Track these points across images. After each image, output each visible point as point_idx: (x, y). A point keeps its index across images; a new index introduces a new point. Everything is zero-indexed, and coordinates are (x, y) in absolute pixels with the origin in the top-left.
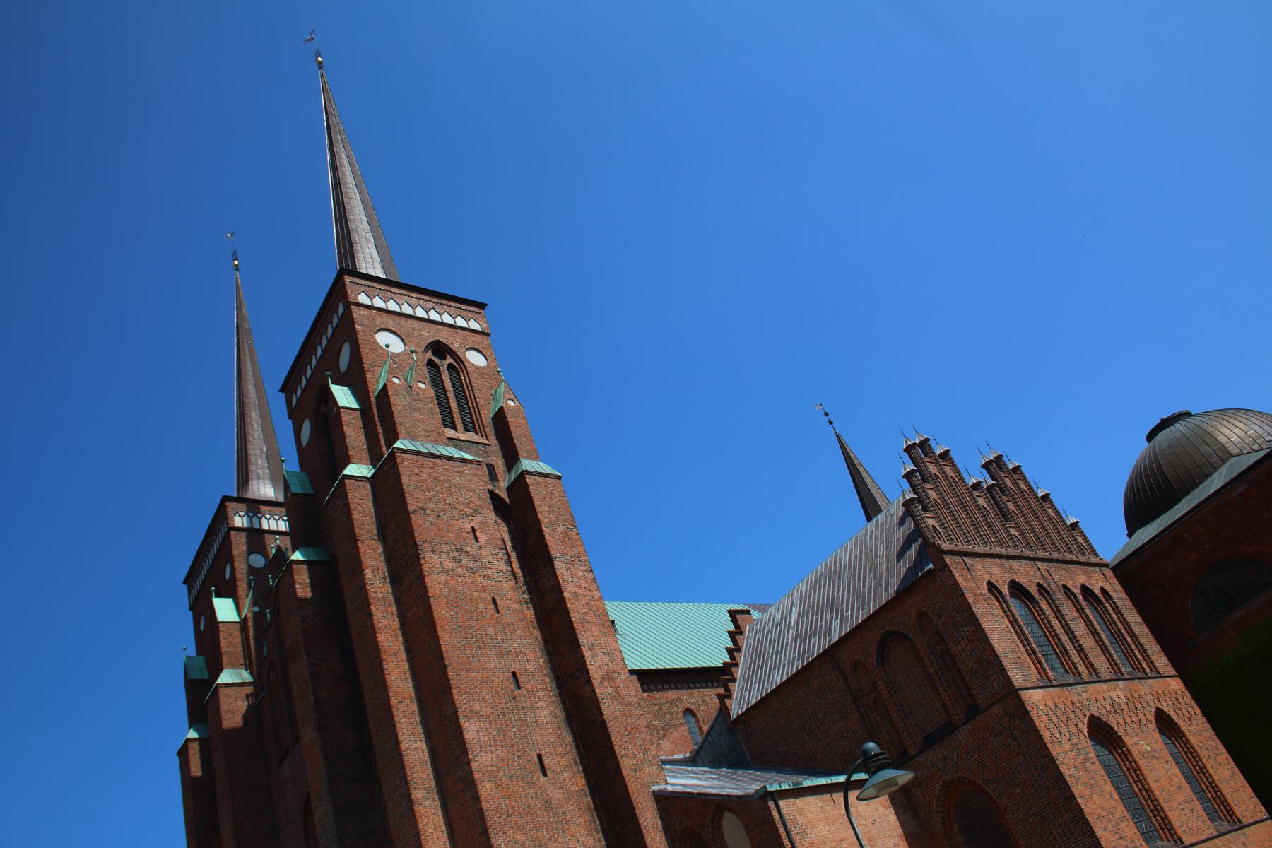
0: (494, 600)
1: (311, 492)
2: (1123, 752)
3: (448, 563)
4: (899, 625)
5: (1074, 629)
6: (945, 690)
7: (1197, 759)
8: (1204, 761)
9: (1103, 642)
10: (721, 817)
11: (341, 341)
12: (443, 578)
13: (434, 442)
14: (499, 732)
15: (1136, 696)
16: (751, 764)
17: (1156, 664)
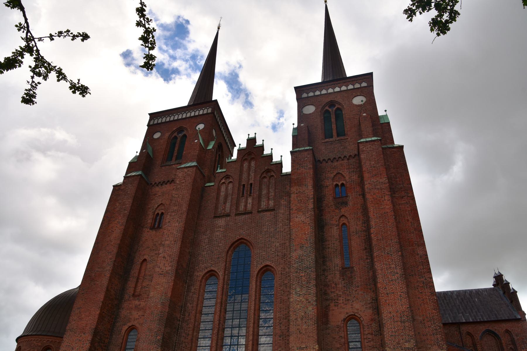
11: (359, 94)
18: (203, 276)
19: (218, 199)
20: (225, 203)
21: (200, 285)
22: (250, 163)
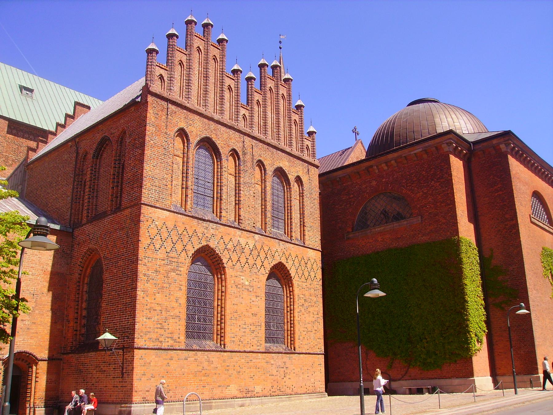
2: (221, 278)
5: (242, 189)
7: (292, 303)
8: (295, 307)
9: (265, 207)
15: (266, 249)
17: (306, 237)
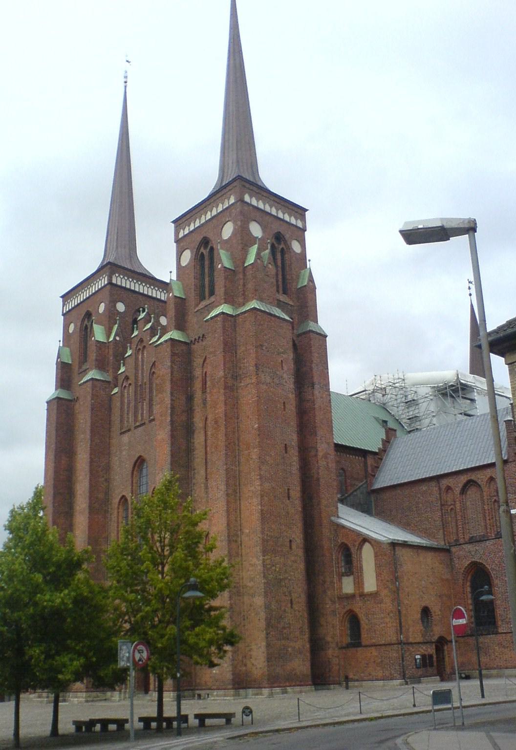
0: (284, 403)
1: (184, 297)
3: (268, 380)
4: (478, 479)
6: (489, 520)
10: (364, 543)
11: (227, 220)
12: (265, 387)
13: (270, 303)
14: (274, 474)
16: (374, 514)
18: (119, 502)
19: (122, 409)
20: (128, 414)
21: (118, 512)
22: (143, 354)
